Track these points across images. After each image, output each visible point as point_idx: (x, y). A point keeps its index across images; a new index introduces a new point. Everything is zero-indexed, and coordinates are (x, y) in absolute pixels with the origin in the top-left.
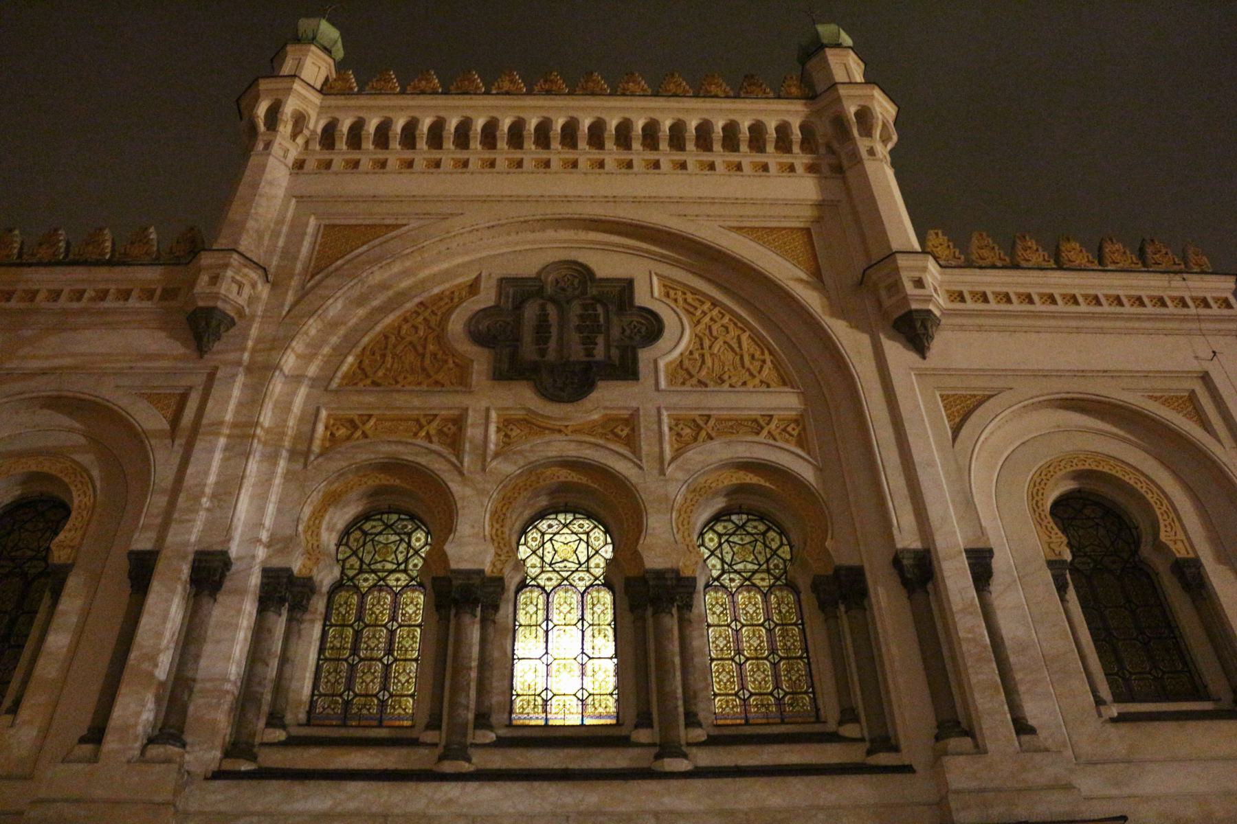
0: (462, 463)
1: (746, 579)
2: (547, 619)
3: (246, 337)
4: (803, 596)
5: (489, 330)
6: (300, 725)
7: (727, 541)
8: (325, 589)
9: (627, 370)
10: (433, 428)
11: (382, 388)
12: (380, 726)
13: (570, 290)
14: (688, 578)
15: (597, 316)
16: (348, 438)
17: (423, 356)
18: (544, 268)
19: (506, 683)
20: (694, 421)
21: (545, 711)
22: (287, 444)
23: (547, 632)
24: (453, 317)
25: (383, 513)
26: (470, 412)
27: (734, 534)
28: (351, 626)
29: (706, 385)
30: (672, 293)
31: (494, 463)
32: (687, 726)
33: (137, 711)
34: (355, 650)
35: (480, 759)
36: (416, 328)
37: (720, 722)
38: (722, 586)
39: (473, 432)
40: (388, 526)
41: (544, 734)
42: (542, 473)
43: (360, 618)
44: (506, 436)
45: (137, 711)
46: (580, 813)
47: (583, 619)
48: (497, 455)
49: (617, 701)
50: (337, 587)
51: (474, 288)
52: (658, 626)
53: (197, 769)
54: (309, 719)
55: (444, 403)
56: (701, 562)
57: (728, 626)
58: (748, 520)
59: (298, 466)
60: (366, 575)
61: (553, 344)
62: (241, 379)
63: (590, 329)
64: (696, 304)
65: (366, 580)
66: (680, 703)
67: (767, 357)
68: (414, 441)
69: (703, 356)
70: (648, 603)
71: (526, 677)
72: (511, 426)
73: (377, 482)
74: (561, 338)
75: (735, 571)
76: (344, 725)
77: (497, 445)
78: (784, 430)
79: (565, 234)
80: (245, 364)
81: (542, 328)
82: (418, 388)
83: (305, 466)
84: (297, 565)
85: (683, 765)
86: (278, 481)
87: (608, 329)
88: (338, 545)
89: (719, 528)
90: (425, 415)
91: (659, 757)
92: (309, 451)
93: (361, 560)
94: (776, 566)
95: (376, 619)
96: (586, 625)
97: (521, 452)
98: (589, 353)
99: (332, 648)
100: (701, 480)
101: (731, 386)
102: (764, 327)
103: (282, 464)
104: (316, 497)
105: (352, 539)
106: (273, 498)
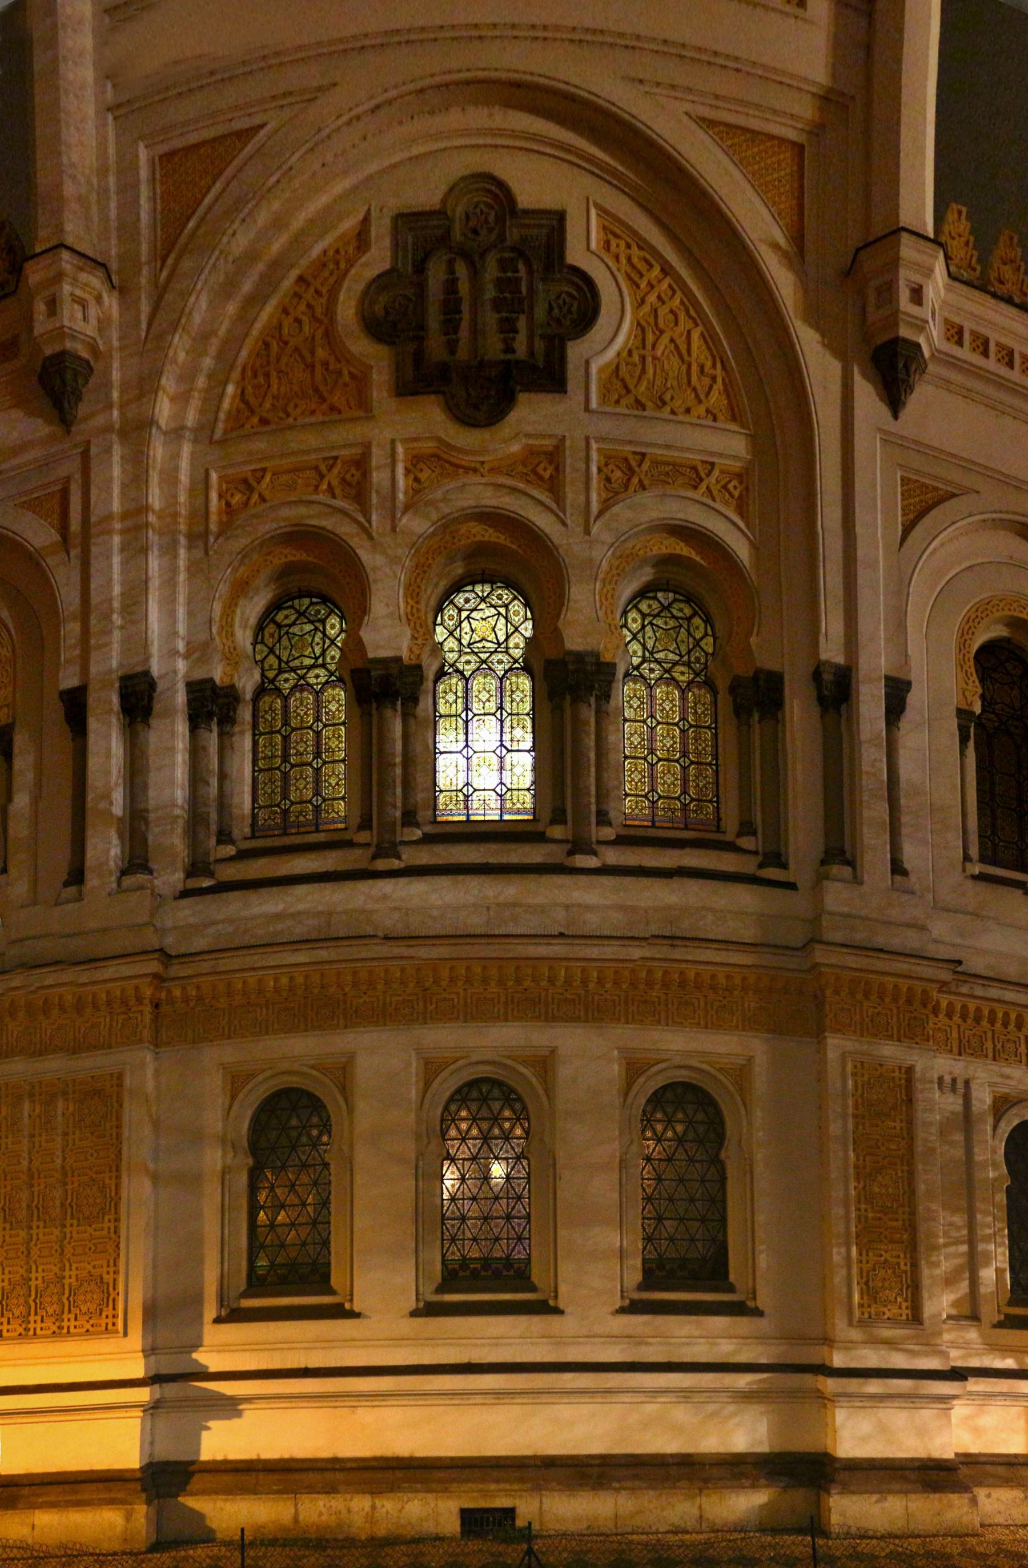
0: (370, 523)
1: (666, 671)
2: (467, 709)
3: (108, 385)
4: (719, 696)
5: (387, 313)
6: (246, 839)
7: (651, 623)
8: (248, 696)
9: (551, 377)
10: (333, 477)
11: (273, 427)
12: (317, 831)
13: (484, 232)
14: (608, 664)
15: (518, 280)
16: (246, 504)
17: (312, 367)
18: (451, 190)
19: (430, 777)
20: (626, 460)
21: (467, 807)
22: (183, 527)
23: (467, 722)
24: (341, 297)
25: (293, 599)
26: (374, 450)
27: (658, 615)
28: (278, 732)
29: (644, 408)
30: (614, 242)
31: (404, 521)
32: (598, 824)
33: (106, 848)
34: (285, 757)
35: (411, 857)
36: (298, 321)
37: (629, 823)
38: (642, 676)
39: (379, 477)
40: (301, 614)
41: (468, 829)
42: (457, 531)
43: (286, 723)
44: (416, 480)
45: (106, 848)
46: (498, 905)
47: (501, 708)
48: (407, 508)
49: (534, 796)
50: (260, 692)
51: (362, 239)
52: (576, 720)
53: (166, 891)
54: (253, 831)
55: (343, 436)
56: (622, 646)
57: (644, 721)
58: (675, 600)
59: (199, 554)
60: (286, 675)
61: (464, 333)
62: (117, 451)
63: (511, 303)
64: (641, 266)
65: (286, 680)
66: (593, 800)
67: (719, 372)
68: (314, 497)
69: (643, 358)
70: (566, 688)
71: (449, 772)
72: (421, 465)
73: (284, 560)
74: (474, 322)
75: (656, 661)
76: (285, 834)
77: (406, 493)
78: (725, 487)
79: (478, 117)
80: (117, 426)
81: (451, 306)
82: (313, 419)
83: (206, 553)
84: (218, 674)
85: (592, 862)
86: (182, 577)
87: (531, 308)
88: (254, 644)
89: (644, 607)
90: (325, 459)
91: (571, 853)
92: (207, 531)
93: (279, 658)
94: (698, 660)
95: (302, 721)
96: (505, 714)
97: (432, 503)
98: (509, 349)
99: (264, 758)
100: (629, 545)
101: (673, 412)
102: (718, 314)
103: (182, 552)
104: (223, 588)
105: (267, 635)
106: (181, 598)
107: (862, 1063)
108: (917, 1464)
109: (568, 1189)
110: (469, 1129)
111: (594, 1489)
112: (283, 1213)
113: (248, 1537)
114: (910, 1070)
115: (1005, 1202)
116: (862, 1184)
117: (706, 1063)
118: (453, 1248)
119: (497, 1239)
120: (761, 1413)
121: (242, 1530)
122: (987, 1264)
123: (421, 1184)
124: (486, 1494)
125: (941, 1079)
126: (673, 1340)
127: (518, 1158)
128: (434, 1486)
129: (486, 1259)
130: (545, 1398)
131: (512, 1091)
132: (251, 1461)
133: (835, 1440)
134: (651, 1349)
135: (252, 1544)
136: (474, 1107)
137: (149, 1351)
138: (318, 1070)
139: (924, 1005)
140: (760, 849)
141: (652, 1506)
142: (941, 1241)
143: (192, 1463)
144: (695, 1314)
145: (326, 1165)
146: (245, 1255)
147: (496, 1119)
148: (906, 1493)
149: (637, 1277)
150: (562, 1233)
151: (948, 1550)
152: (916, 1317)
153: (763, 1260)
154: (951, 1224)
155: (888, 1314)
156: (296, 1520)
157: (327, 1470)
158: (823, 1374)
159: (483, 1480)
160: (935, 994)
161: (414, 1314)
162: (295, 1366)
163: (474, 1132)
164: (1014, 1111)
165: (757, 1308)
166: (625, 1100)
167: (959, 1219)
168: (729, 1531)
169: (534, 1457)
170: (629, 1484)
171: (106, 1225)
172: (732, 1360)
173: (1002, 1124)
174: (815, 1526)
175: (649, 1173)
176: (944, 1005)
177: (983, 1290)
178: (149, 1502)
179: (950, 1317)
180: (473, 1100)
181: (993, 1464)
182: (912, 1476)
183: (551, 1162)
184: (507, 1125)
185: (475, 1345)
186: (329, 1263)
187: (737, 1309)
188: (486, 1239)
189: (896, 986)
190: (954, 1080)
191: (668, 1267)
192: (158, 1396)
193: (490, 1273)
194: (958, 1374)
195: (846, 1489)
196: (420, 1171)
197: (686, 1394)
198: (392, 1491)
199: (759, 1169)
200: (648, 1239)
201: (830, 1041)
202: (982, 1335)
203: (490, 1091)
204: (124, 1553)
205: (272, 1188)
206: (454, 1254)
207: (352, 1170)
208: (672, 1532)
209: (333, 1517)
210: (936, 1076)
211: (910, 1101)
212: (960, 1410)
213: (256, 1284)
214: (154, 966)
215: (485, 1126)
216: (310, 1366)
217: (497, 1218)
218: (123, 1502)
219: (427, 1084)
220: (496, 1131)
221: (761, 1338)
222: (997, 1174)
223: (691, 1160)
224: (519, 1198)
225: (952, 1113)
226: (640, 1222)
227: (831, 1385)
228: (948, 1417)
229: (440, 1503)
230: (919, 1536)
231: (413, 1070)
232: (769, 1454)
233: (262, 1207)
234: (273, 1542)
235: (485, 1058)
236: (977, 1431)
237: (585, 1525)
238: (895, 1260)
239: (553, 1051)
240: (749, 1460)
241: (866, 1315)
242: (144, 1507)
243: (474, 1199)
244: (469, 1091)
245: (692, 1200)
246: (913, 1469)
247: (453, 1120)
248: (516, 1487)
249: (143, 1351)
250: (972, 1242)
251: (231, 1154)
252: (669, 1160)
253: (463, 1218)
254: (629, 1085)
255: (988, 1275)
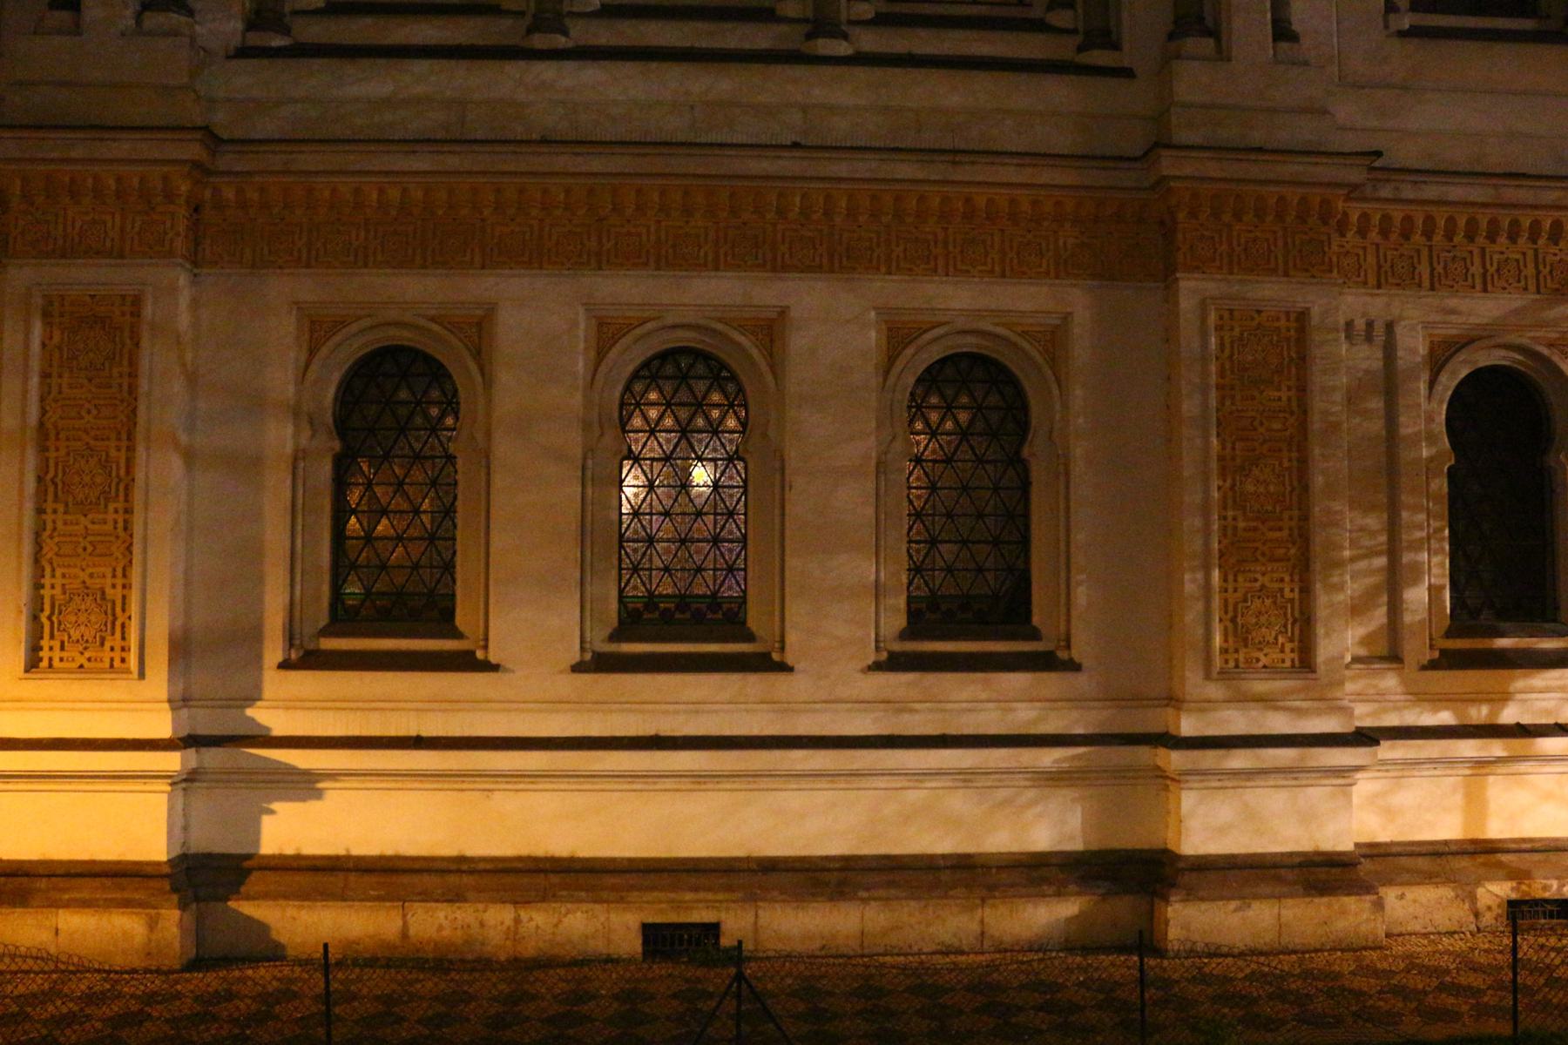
107: (1231, 311)
108: (1297, 860)
109: (800, 505)
110: (661, 417)
111: (831, 899)
112: (384, 521)
113: (334, 955)
114: (1303, 316)
115: (1445, 489)
116: (1228, 484)
117: (1003, 325)
118: (636, 581)
119: (699, 570)
120: (1073, 800)
121: (326, 946)
122: (1416, 581)
123: (589, 491)
124: (678, 906)
125: (1349, 325)
126: (949, 706)
127: (730, 459)
128: (605, 895)
129: (682, 597)
130: (764, 783)
131: (723, 366)
132: (337, 858)
133: (1180, 833)
134: (917, 717)
135: (339, 964)
136: (668, 388)
137: (180, 702)
138: (441, 324)
139: (1324, 220)
140: (1081, 29)
141: (913, 921)
142: (1347, 553)
143: (249, 857)
144: (982, 670)
145: (450, 459)
146: (327, 577)
147: (699, 406)
148: (1279, 897)
149: (901, 622)
150: (792, 562)
151: (1337, 968)
152: (1305, 662)
153: (1081, 595)
154: (1362, 529)
155: (1264, 660)
156: (404, 935)
157: (450, 871)
158: (1165, 746)
159: (675, 888)
160: (1340, 205)
161: (578, 668)
162: (402, 733)
163: (668, 422)
164: (1462, 356)
165: (1071, 659)
166: (885, 380)
167: (1374, 521)
168: (1022, 951)
169: (748, 859)
170: (882, 893)
171: (111, 516)
172: (1033, 731)
173: (1443, 378)
174: (1147, 943)
175: (918, 479)
176: (1354, 218)
177: (1408, 618)
178: (183, 907)
179: (1356, 660)
180: (667, 378)
181: (1411, 855)
182: (1290, 875)
183: (777, 465)
184: (715, 413)
185: (666, 712)
186: (454, 595)
187: (1044, 662)
188: (683, 569)
189: (1282, 199)
190: (1370, 325)
191: (944, 607)
192: (193, 764)
193: (688, 615)
194: (1365, 737)
195: (1191, 895)
196: (589, 474)
197: (966, 777)
198: (543, 900)
199: (1078, 468)
200: (916, 570)
201: (1182, 284)
202: (1404, 682)
203: (692, 366)
204: (147, 971)
205: (369, 485)
206: (637, 589)
207: (488, 467)
208: (941, 953)
209: (459, 933)
210: (1342, 322)
211: (1303, 359)
212: (1365, 786)
213: (343, 618)
214: (194, 150)
215: (683, 414)
216: (424, 734)
217: (699, 541)
218: (142, 905)
219: (601, 354)
220: (700, 422)
221: (1077, 701)
222: (1434, 450)
223: (980, 461)
224: (731, 514)
225: (1367, 372)
226: (904, 547)
227: (1176, 760)
228: (1348, 797)
229: (613, 916)
230: (1295, 952)
231: (581, 334)
232: (1083, 853)
233: (354, 512)
234: (372, 962)
235: (685, 321)
236: (1389, 813)
237: (818, 944)
238: (1276, 585)
239: (783, 312)
240: (1054, 861)
241: (1232, 664)
242: (176, 913)
243: (666, 514)
244: (662, 365)
245: (980, 516)
246: (1292, 867)
247: (638, 405)
248: (720, 896)
249: (169, 701)
250: (1393, 552)
251: (306, 433)
252: (948, 460)
253: (651, 540)
254: (891, 360)
255: (1416, 597)
